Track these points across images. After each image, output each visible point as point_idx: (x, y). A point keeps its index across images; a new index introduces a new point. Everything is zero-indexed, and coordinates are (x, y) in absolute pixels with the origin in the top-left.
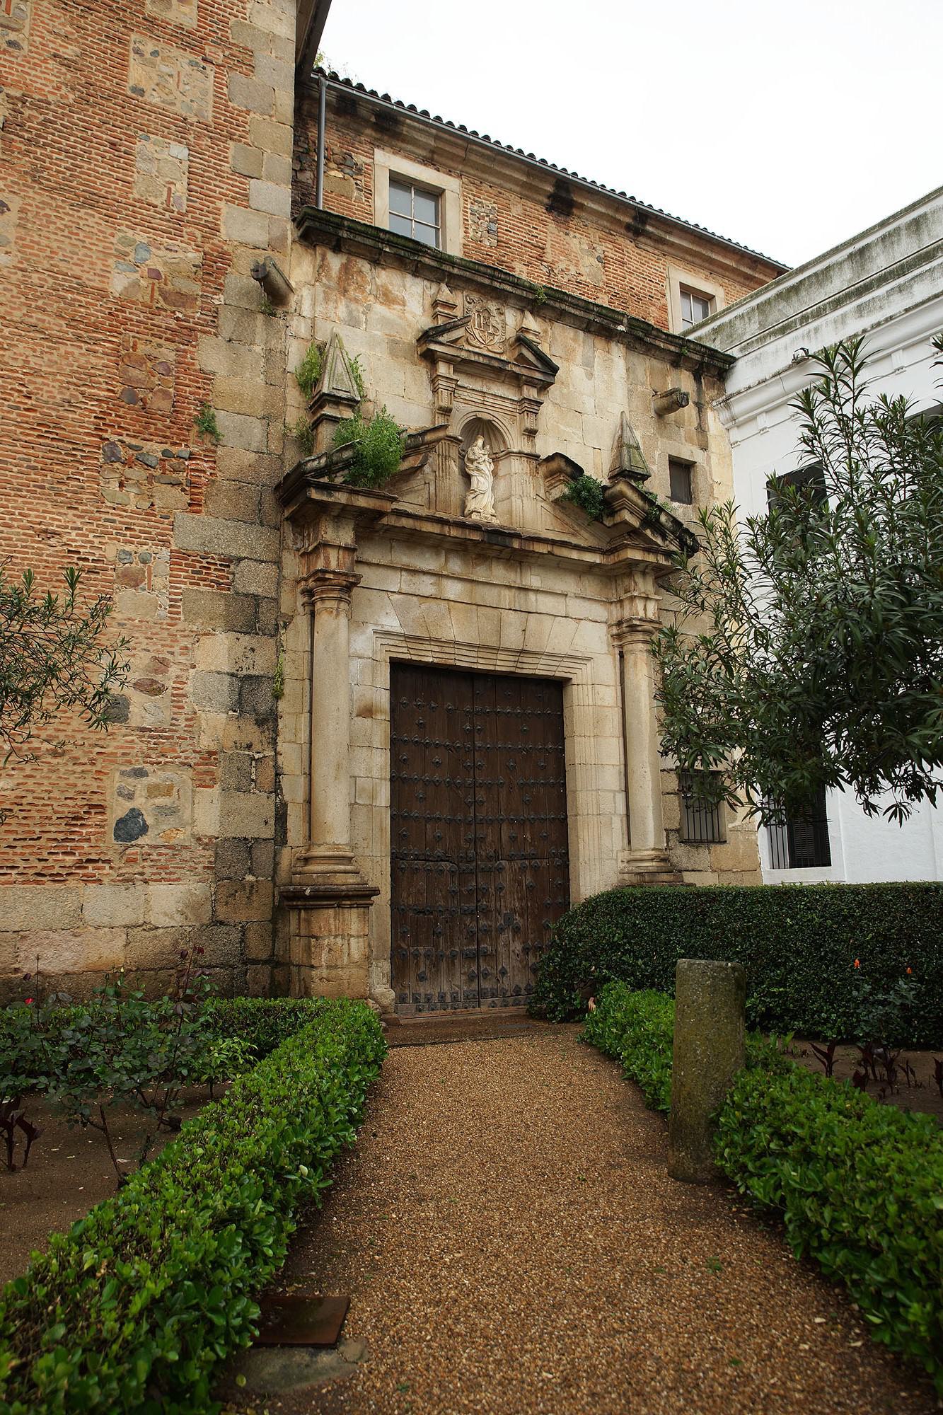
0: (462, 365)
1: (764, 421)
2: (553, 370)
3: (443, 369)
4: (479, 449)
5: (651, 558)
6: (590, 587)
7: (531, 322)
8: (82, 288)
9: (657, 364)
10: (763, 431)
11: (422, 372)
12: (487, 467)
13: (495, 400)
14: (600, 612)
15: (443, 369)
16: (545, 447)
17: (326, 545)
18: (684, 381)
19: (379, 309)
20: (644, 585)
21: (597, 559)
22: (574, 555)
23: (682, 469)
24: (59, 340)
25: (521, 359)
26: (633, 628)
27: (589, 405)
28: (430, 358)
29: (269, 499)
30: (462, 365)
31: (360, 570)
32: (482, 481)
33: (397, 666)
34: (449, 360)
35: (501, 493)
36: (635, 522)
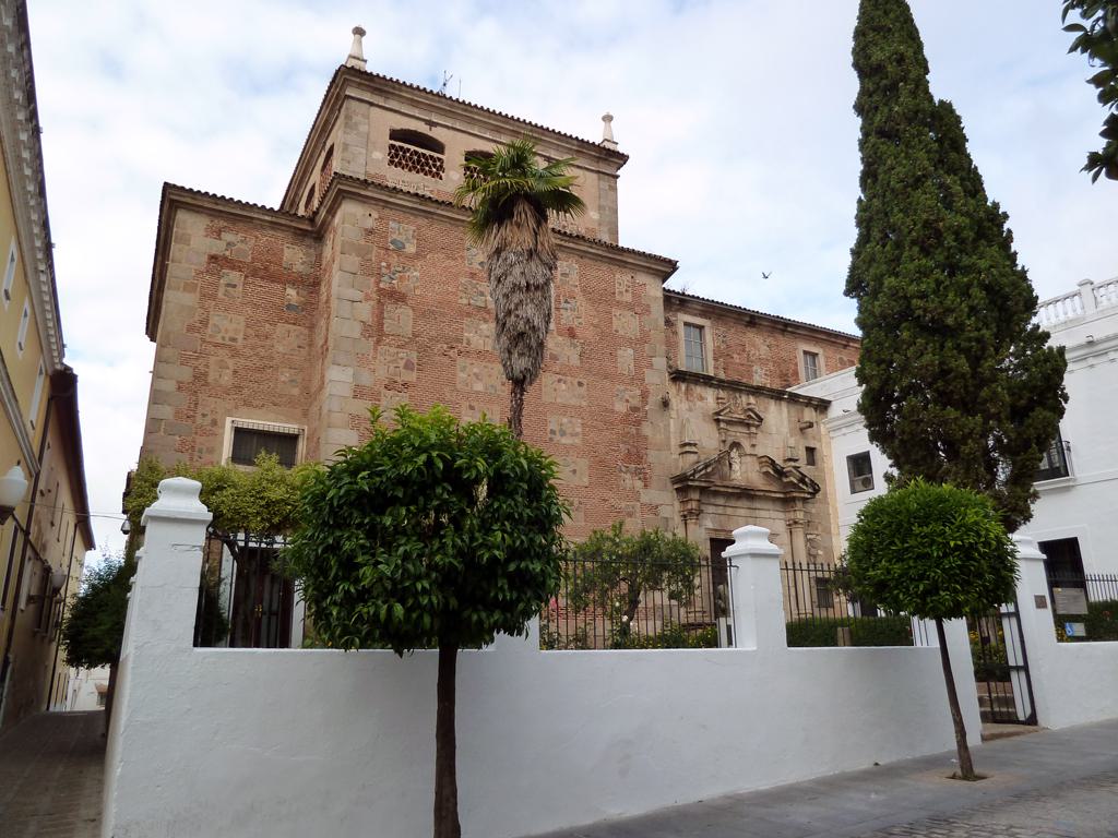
0: (729, 423)
1: (844, 430)
2: (761, 420)
3: (722, 425)
4: (734, 454)
5: (802, 495)
6: (778, 506)
7: (752, 400)
8: (606, 410)
9: (799, 407)
10: (844, 435)
11: (714, 426)
12: (738, 461)
13: (738, 433)
14: (781, 515)
15: (722, 425)
16: (760, 451)
17: (691, 500)
18: (809, 414)
19: (699, 403)
20: (799, 505)
21: (782, 496)
22: (773, 495)
23: (811, 451)
24: (602, 430)
25: (749, 416)
26: (796, 523)
27: (774, 430)
28: (718, 421)
29: (668, 481)
30: (729, 423)
31: (703, 507)
32: (736, 467)
33: (712, 540)
34: (723, 421)
35: (744, 471)
36: (795, 481)
